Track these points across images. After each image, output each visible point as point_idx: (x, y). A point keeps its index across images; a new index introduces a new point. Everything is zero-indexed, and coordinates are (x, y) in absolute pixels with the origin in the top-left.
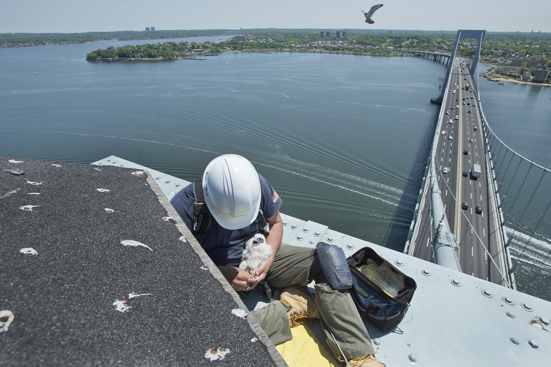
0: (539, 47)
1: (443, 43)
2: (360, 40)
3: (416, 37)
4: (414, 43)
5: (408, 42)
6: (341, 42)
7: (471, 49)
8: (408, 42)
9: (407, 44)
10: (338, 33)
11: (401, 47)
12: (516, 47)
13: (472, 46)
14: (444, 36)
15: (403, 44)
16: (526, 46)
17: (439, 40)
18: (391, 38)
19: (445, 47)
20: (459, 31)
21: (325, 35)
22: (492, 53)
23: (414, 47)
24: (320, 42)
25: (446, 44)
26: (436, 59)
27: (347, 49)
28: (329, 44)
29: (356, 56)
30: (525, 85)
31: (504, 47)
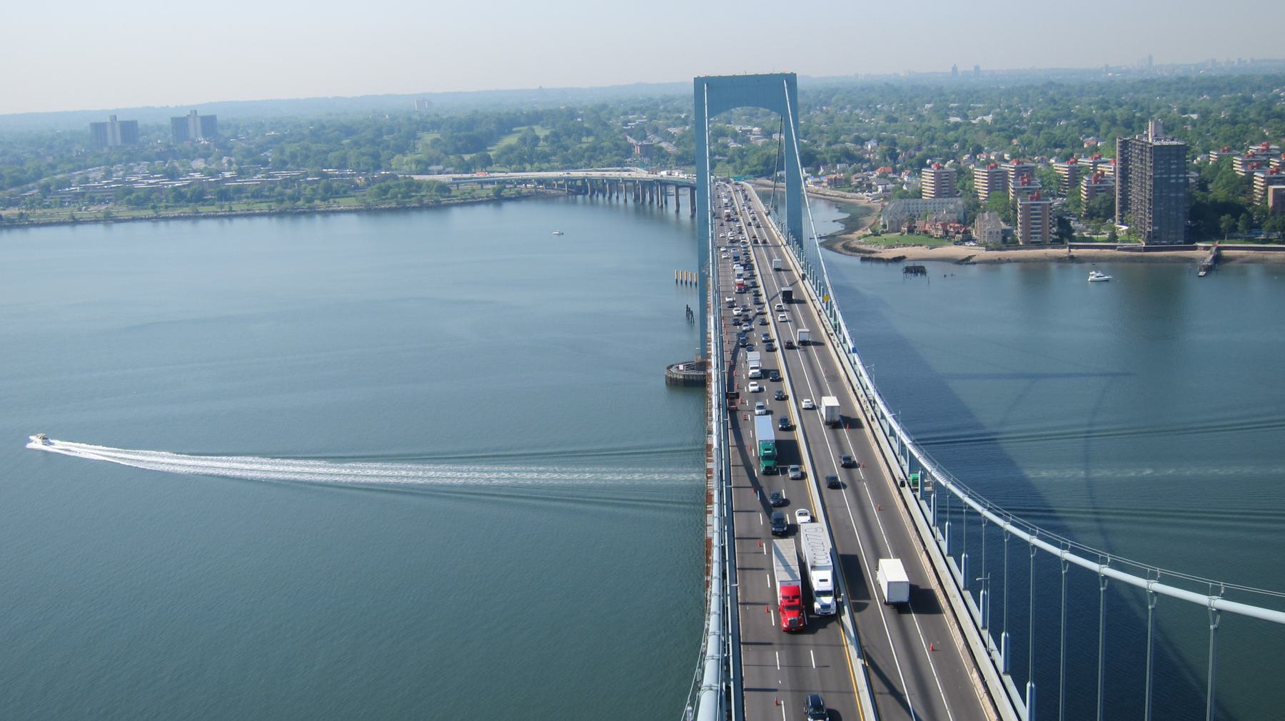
0: (995, 121)
1: (656, 131)
2: (289, 149)
3: (536, 118)
4: (537, 139)
5: (511, 140)
6: (199, 164)
7: (765, 145)
8: (511, 140)
9: (511, 149)
10: (180, 124)
11: (487, 163)
12: (925, 125)
13: (768, 134)
14: (653, 109)
15: (493, 152)
16: (953, 120)
17: (637, 120)
18: (435, 126)
19: (668, 147)
20: (699, 82)
21: (114, 138)
22: (849, 157)
23: (545, 158)
24: (96, 174)
25: (669, 137)
26: (646, 200)
27: (239, 190)
28: (141, 180)
29: (287, 222)
30: (999, 261)
31: (884, 129)
